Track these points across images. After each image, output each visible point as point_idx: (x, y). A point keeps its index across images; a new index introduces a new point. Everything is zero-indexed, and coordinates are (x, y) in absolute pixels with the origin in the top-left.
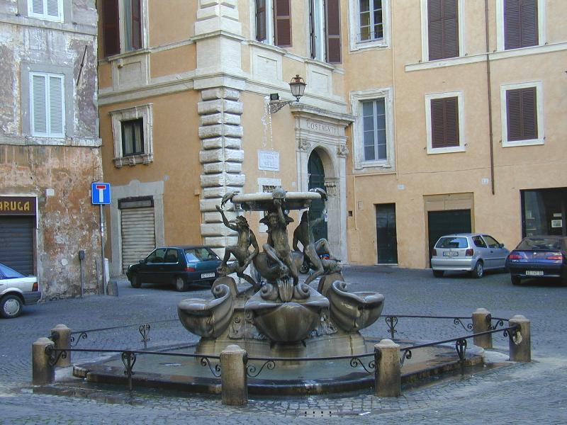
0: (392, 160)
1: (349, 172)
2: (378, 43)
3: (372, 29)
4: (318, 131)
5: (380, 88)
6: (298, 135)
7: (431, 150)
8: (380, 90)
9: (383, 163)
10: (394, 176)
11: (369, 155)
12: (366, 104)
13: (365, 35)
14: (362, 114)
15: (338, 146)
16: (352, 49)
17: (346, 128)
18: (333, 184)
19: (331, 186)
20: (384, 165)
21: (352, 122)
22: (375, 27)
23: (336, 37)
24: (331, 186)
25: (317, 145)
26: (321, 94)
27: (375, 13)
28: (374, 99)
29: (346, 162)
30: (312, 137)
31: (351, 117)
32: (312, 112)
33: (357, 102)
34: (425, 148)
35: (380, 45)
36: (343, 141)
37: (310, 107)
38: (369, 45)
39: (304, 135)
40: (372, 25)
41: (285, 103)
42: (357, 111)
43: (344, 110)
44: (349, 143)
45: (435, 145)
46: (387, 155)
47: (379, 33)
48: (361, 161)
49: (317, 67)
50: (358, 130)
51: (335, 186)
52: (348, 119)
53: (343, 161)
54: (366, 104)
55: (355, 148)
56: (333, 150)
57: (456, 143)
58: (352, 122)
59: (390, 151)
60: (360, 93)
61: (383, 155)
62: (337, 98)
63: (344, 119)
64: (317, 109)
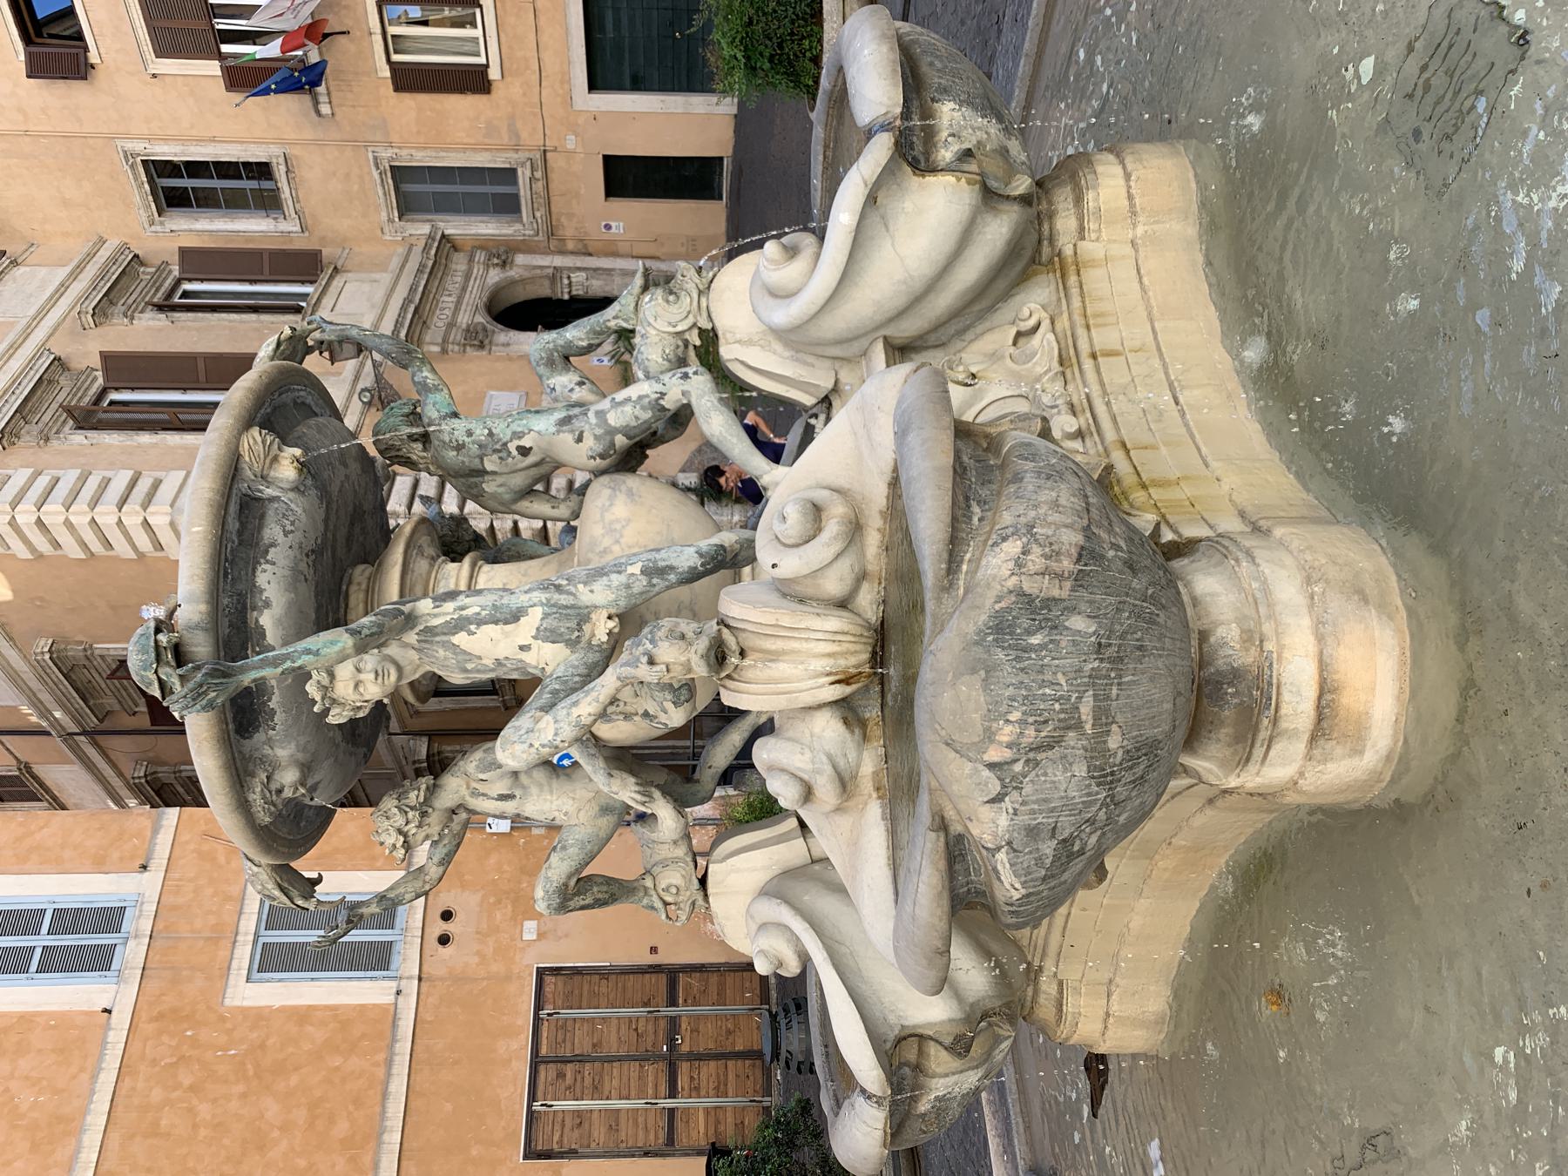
1: (547, 251)
2: (280, 172)
3: (253, 184)
4: (452, 306)
5: (370, 173)
6: (456, 348)
8: (376, 174)
9: (523, 175)
10: (548, 154)
11: (508, 206)
12: (407, 206)
13: (269, 203)
14: (430, 217)
15: (488, 266)
16: (298, 228)
17: (455, 248)
18: (566, 281)
19: (570, 285)
20: (528, 173)
21: (443, 236)
23: (266, 257)
24: (570, 285)
25: (483, 311)
26: (380, 294)
27: (221, 176)
28: (397, 189)
29: (524, 252)
30: (464, 319)
31: (431, 237)
32: (409, 316)
35: (283, 168)
37: (398, 324)
38: (286, 194)
39: (456, 335)
41: (378, 378)
42: (420, 229)
43: (418, 249)
44: (484, 244)
46: (508, 166)
47: (262, 170)
48: (521, 222)
49: (324, 301)
50: (457, 226)
51: (569, 277)
52: (436, 244)
53: (520, 259)
54: (407, 206)
56: (495, 276)
59: (499, 162)
60: (384, 215)
61: (509, 175)
62: (395, 263)
63: (433, 252)
64: (404, 308)
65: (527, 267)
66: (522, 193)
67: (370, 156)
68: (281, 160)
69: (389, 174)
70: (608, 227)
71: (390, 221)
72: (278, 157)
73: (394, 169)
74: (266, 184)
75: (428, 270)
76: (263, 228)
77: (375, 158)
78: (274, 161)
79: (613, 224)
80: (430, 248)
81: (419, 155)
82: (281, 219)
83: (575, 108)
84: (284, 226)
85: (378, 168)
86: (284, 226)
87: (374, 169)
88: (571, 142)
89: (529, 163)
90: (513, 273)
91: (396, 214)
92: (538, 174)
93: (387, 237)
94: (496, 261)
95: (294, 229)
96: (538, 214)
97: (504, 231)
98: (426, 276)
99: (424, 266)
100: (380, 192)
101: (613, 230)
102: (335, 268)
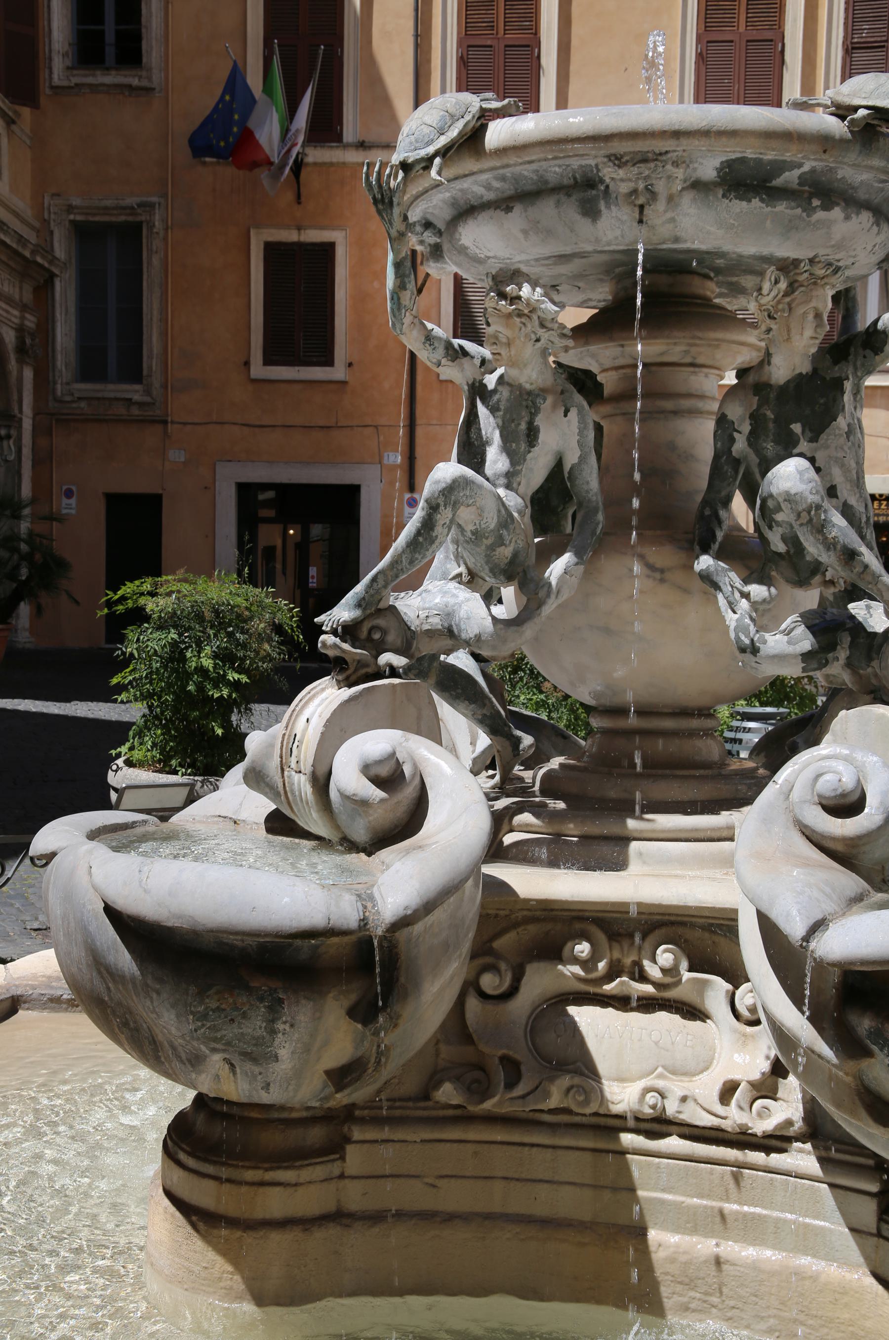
0: (156, 382)
1: (37, 413)
3: (110, 37)
7: (258, 370)
9: (135, 392)
14: (73, 261)
16: (56, 81)
20: (136, 397)
22: (118, 33)
31: (53, 260)
33: (67, 223)
34: (247, 364)
35: (135, 82)
36: (31, 321)
40: (110, 28)
45: (269, 360)
46: (145, 372)
52: (46, 265)
53: (28, 374)
55: (58, 347)
57: (328, 361)
58: (52, 276)
59: (151, 361)
60: (76, 201)
65: (20, 379)
66: (111, 387)
67: (154, 199)
68: (145, 83)
69: (130, 219)
70: (69, 494)
71: (70, 209)
72: (150, 79)
73: (138, 226)
74: (110, 52)
75: (20, 249)
76: (56, 34)
77: (152, 205)
78: (144, 73)
79: (73, 501)
80: (43, 257)
81: (156, 261)
82: (68, 63)
83: (217, 463)
84: (58, 65)
85: (140, 205)
86: (58, 65)
87: (138, 200)
88: (177, 456)
89: (148, 399)
90: (13, 363)
91: (79, 218)
92: (135, 411)
93: (47, 200)
94: (28, 341)
95: (55, 76)
96: (83, 404)
97: (59, 357)
98: (14, 245)
99: (24, 246)
100: (108, 203)
101: (65, 501)
102: (14, 122)
